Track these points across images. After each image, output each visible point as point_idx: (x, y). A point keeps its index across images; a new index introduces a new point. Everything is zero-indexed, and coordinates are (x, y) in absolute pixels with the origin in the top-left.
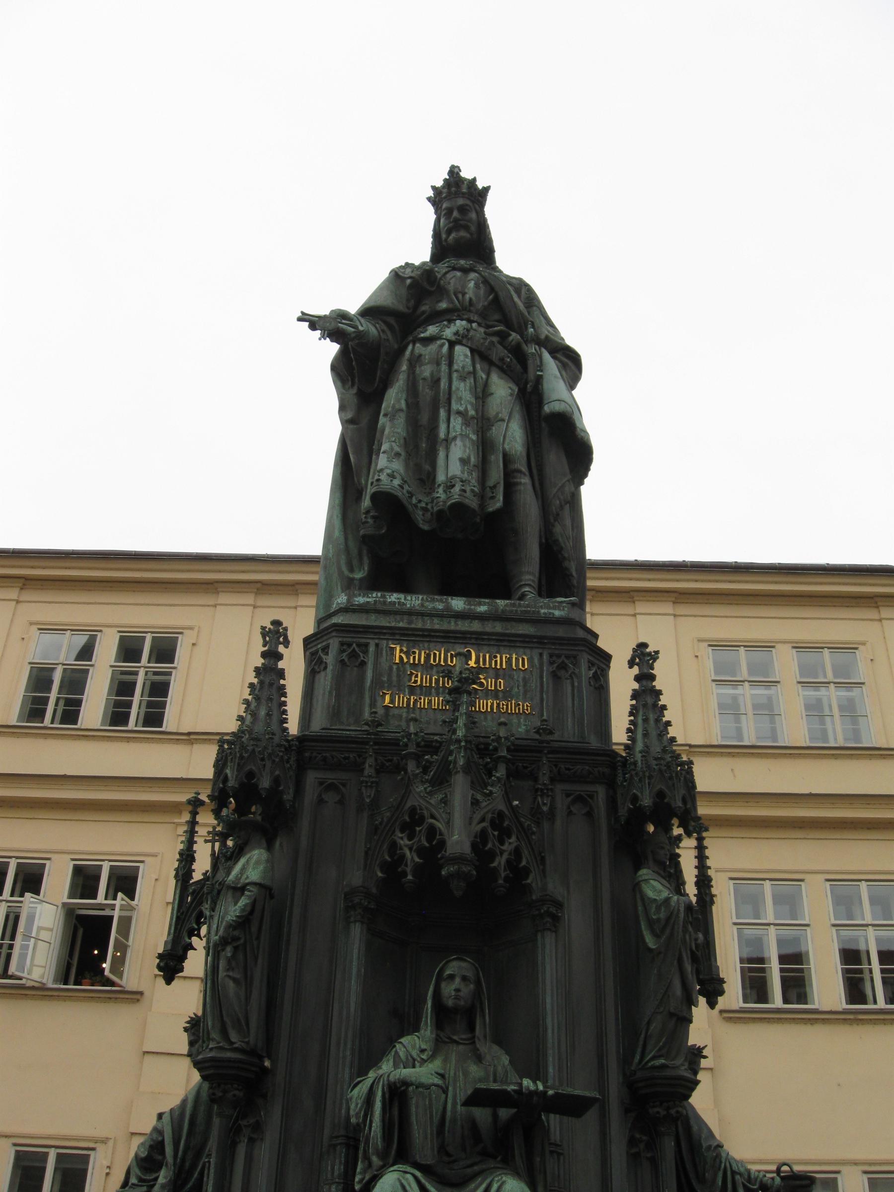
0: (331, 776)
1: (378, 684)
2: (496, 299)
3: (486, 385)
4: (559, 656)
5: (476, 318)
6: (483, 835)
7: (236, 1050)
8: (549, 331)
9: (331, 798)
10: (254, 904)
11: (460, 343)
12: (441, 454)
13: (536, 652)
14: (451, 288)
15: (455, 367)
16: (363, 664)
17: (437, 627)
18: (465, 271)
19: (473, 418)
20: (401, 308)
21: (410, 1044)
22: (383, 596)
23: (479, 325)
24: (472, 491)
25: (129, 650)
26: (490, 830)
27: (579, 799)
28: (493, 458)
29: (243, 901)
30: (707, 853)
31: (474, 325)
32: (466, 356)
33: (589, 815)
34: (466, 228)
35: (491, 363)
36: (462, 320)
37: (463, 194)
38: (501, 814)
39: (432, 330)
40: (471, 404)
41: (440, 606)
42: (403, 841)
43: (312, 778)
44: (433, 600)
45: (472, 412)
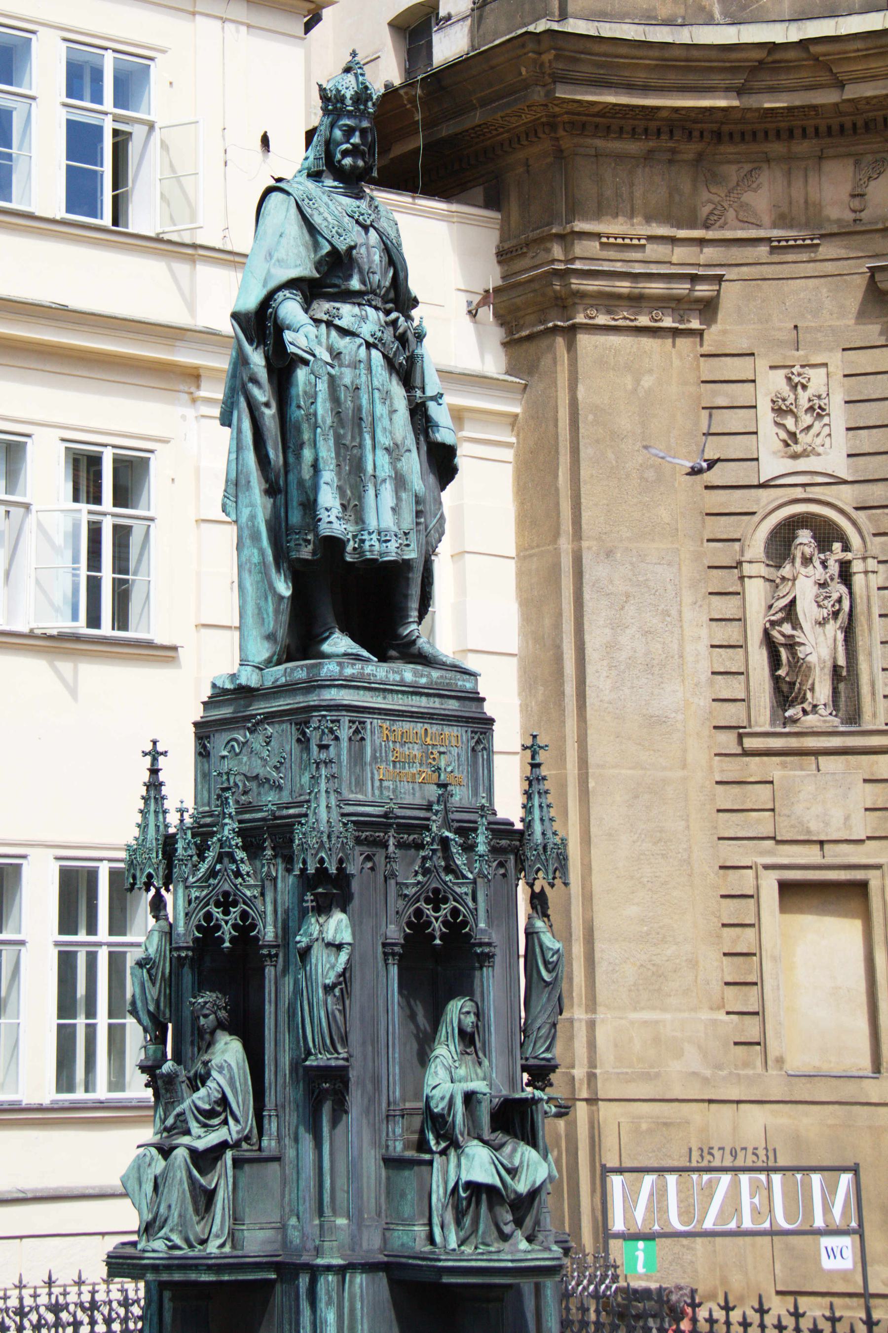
1: (374, 758)
4: (476, 733)
5: (378, 302)
11: (375, 346)
12: (371, 492)
15: (376, 383)
16: (363, 739)
17: (401, 702)
22: (362, 668)
28: (404, 496)
36: (370, 306)
41: (398, 678)
42: (428, 910)
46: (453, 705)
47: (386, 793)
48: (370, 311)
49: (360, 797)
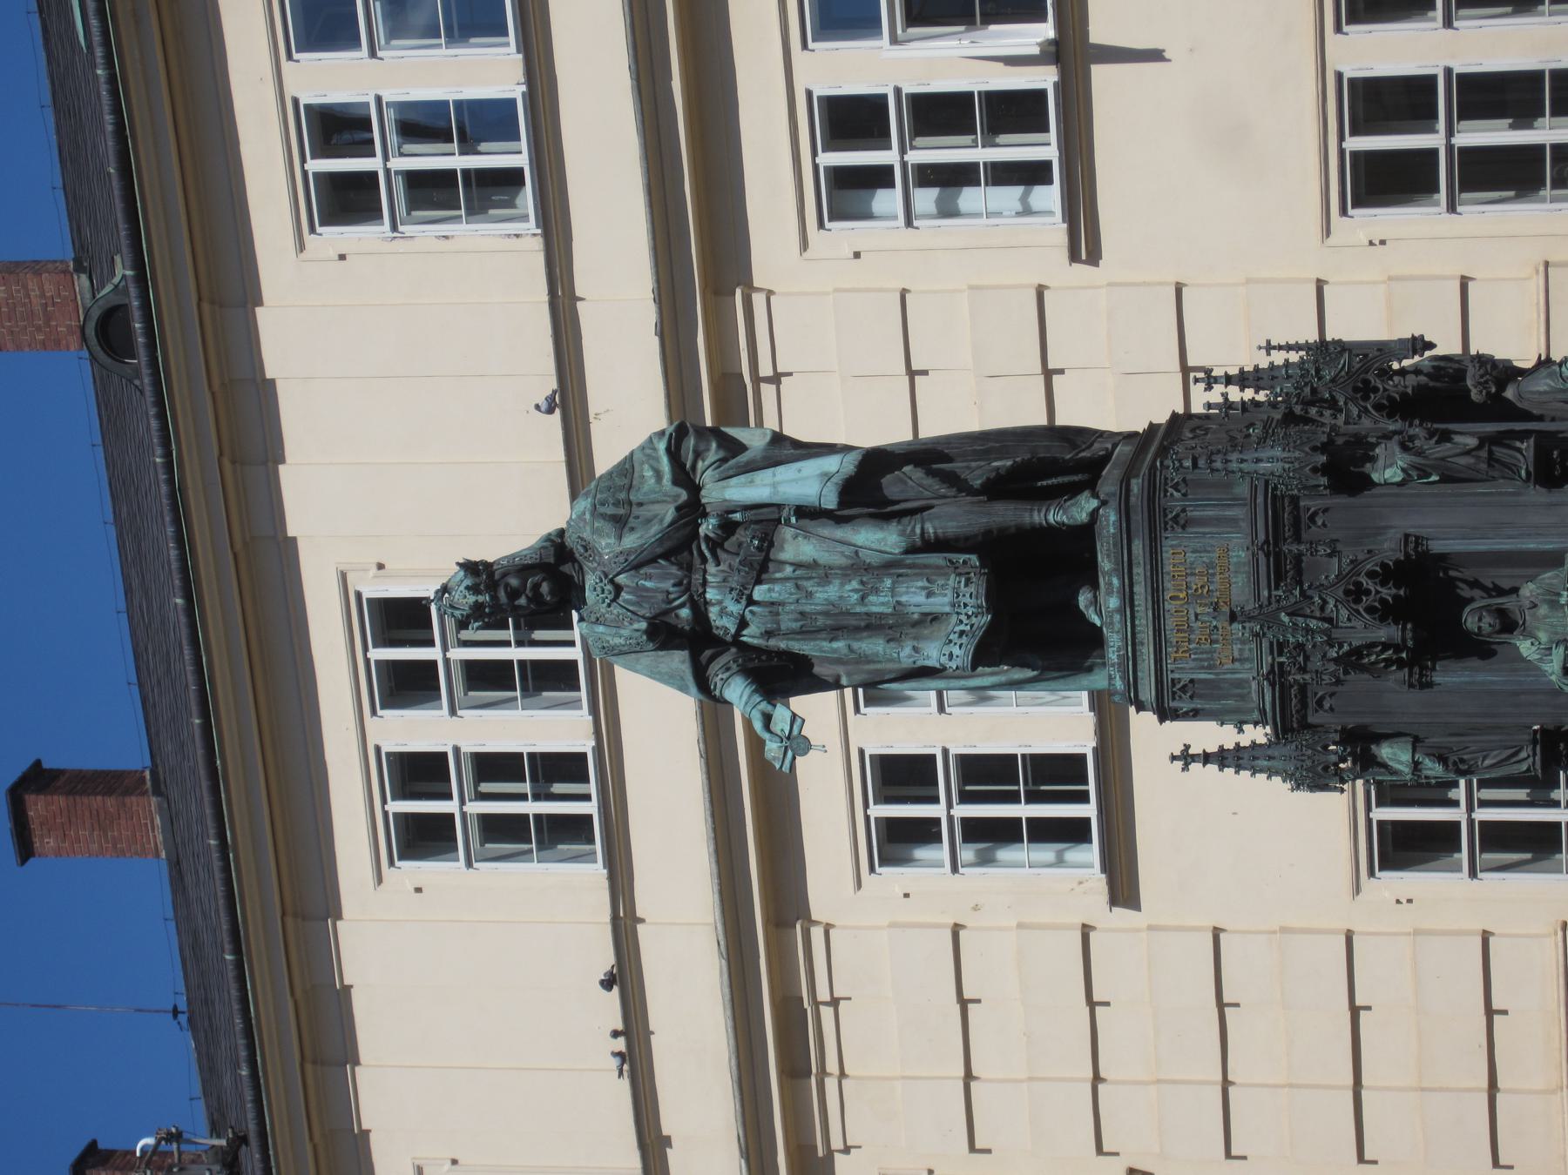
0: (1312, 703)
1: (1210, 667)
2: (661, 556)
3: (798, 565)
6: (1370, 610)
7: (1535, 754)
8: (658, 475)
9: (1327, 705)
10: (1428, 755)
11: (750, 597)
12: (913, 609)
13: (1164, 542)
14: (664, 606)
16: (1192, 681)
18: (618, 589)
19: (862, 583)
20: (684, 654)
21: (1525, 648)
23: (705, 571)
24: (966, 585)
25: (408, 686)
26: (1364, 604)
27: (1312, 518)
29: (1428, 763)
30: (1292, 342)
31: (709, 578)
32: (770, 590)
33: (1326, 510)
34: (536, 587)
35: (767, 560)
37: (492, 598)
38: (1347, 593)
39: (722, 621)
40: (842, 585)
41: (1117, 617)
43: (1311, 719)
44: (1112, 623)
45: (855, 584)
46: (1138, 547)
47: (1246, 654)
48: (711, 594)
49: (1254, 685)
